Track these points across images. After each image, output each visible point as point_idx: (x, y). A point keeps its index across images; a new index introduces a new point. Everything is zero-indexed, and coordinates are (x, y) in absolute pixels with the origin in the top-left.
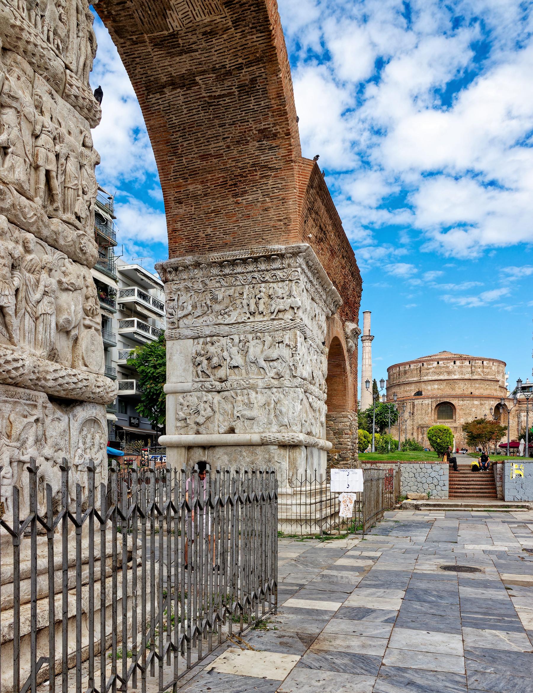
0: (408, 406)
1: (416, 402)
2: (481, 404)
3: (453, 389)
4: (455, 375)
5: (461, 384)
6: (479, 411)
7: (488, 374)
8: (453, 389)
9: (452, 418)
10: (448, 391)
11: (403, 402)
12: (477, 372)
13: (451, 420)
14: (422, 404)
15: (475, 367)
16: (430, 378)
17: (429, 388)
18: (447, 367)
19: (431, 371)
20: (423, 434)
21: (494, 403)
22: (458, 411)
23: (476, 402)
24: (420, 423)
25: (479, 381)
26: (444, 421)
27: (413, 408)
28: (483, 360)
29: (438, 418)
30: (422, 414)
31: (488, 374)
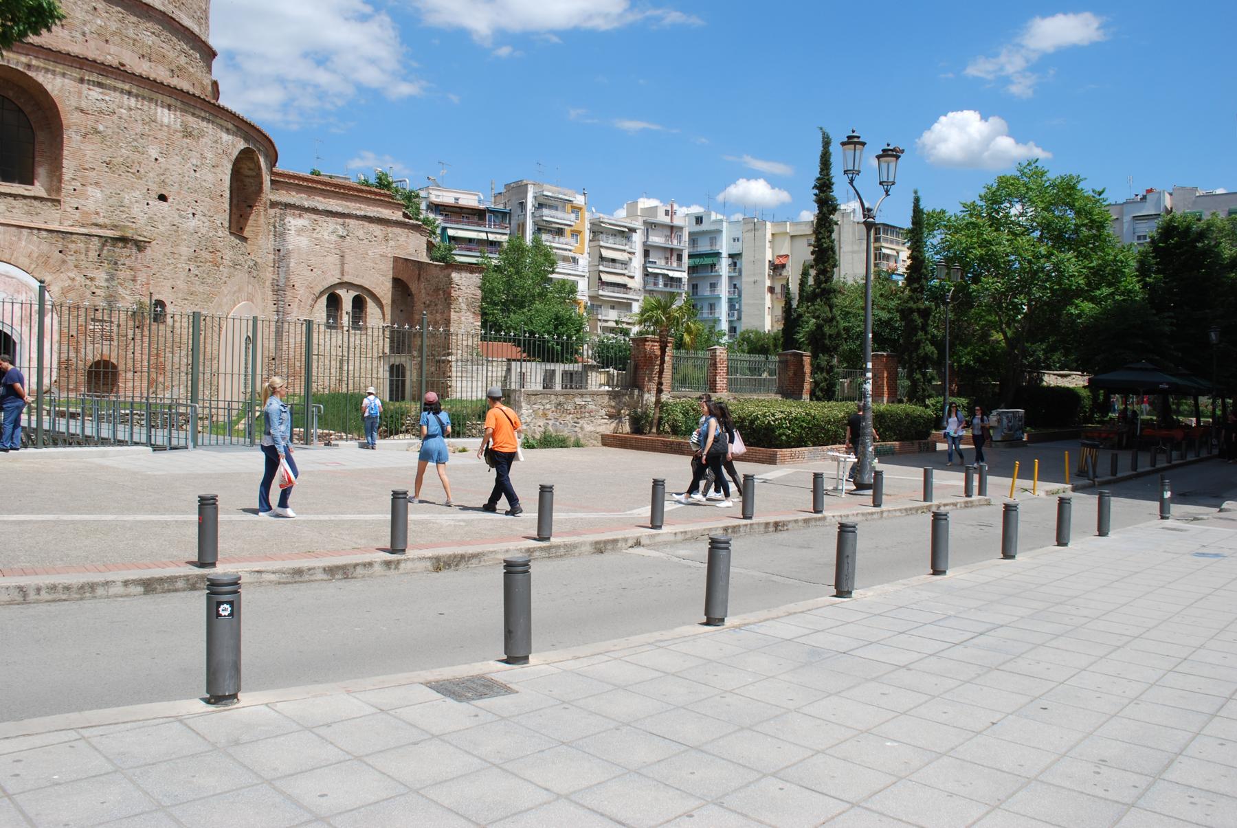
2: (187, 133)
23: (165, 116)
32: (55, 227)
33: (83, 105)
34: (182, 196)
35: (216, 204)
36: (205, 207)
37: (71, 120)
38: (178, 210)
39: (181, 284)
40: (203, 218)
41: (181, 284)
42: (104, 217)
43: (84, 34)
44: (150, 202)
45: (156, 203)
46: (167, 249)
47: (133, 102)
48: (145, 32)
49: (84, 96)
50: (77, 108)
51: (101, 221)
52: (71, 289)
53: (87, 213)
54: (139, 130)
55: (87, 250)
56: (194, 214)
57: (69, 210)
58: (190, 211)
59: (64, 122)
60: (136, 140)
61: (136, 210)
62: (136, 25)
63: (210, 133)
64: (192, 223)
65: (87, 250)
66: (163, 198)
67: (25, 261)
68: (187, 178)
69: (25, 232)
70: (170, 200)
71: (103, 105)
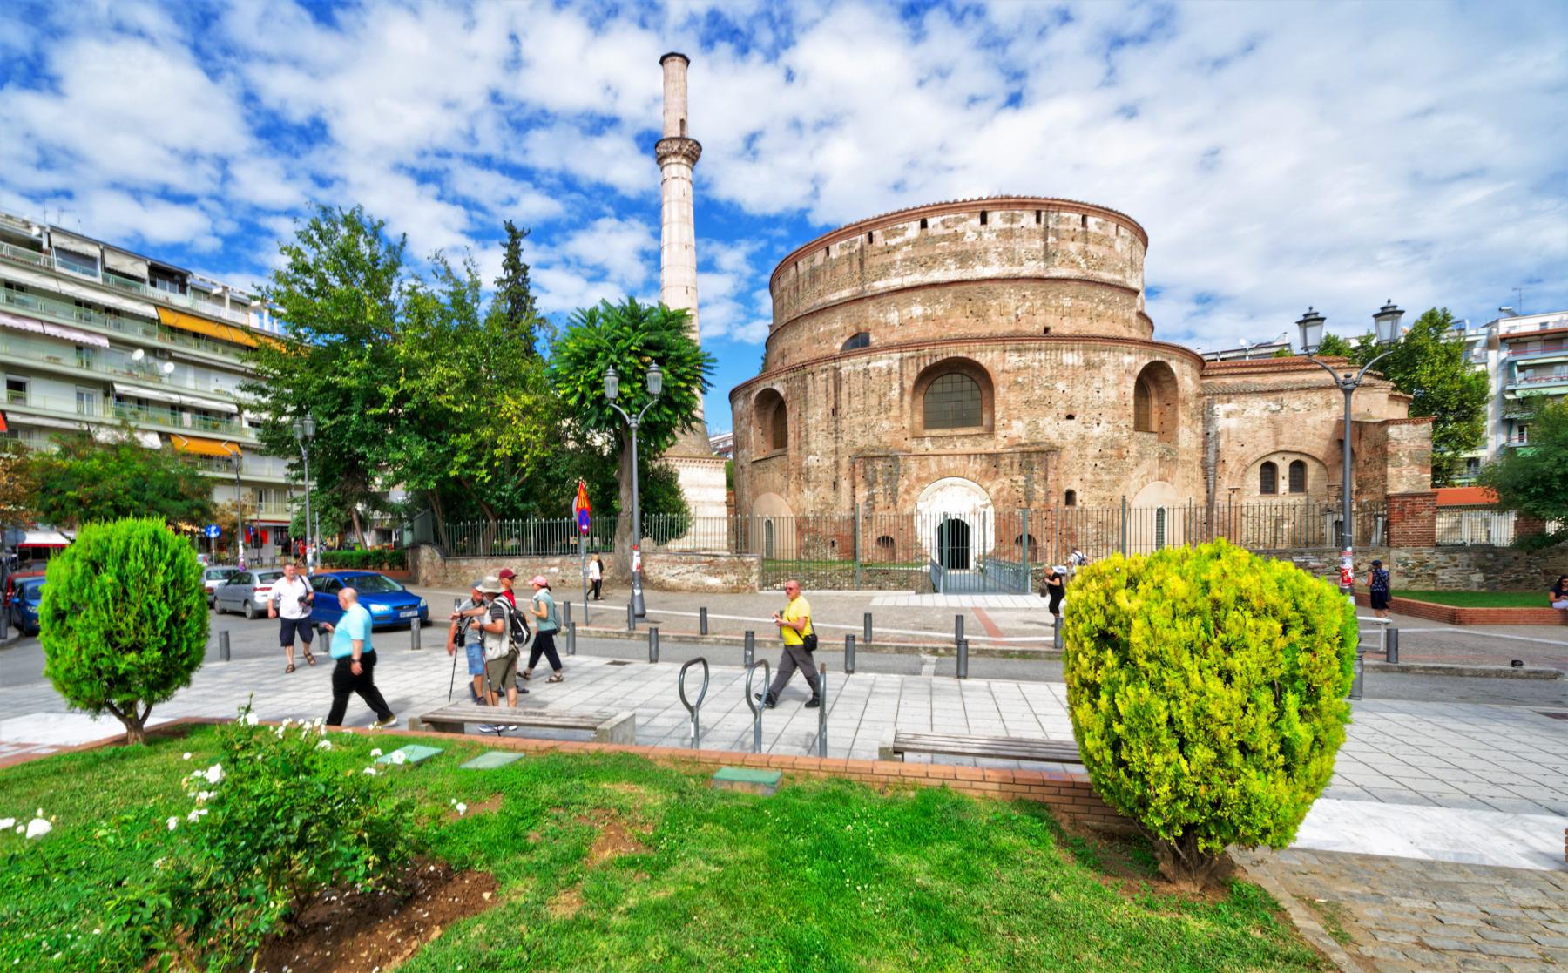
0: (821, 386)
1: (847, 367)
2: (1089, 365)
3: (980, 316)
4: (986, 264)
5: (1010, 298)
6: (1079, 393)
8: (980, 316)
9: (977, 422)
10: (962, 324)
11: (801, 370)
12: (1066, 254)
13: (973, 431)
14: (867, 372)
15: (1057, 233)
16: (895, 282)
17: (893, 317)
18: (957, 237)
20: (871, 484)
21: (1137, 361)
22: (1001, 392)
23: (1071, 358)
24: (861, 442)
25: (1074, 287)
26: (948, 432)
27: (837, 388)
28: (1085, 210)
29: (929, 424)
30: (866, 411)
32: (991, 450)
33: (1007, 368)
35: (1120, 412)
37: (999, 380)
39: (1088, 476)
41: (1088, 476)
43: (1017, 316)
46: (1075, 453)
47: (1043, 356)
51: (1023, 441)
52: (1002, 489)
54: (1048, 373)
55: (1012, 463)
58: (1095, 422)
59: (994, 382)
61: (1049, 430)
62: (1057, 297)
64: (1097, 431)
65: (1012, 463)
66: (1070, 417)
67: (972, 475)
71: (1021, 364)
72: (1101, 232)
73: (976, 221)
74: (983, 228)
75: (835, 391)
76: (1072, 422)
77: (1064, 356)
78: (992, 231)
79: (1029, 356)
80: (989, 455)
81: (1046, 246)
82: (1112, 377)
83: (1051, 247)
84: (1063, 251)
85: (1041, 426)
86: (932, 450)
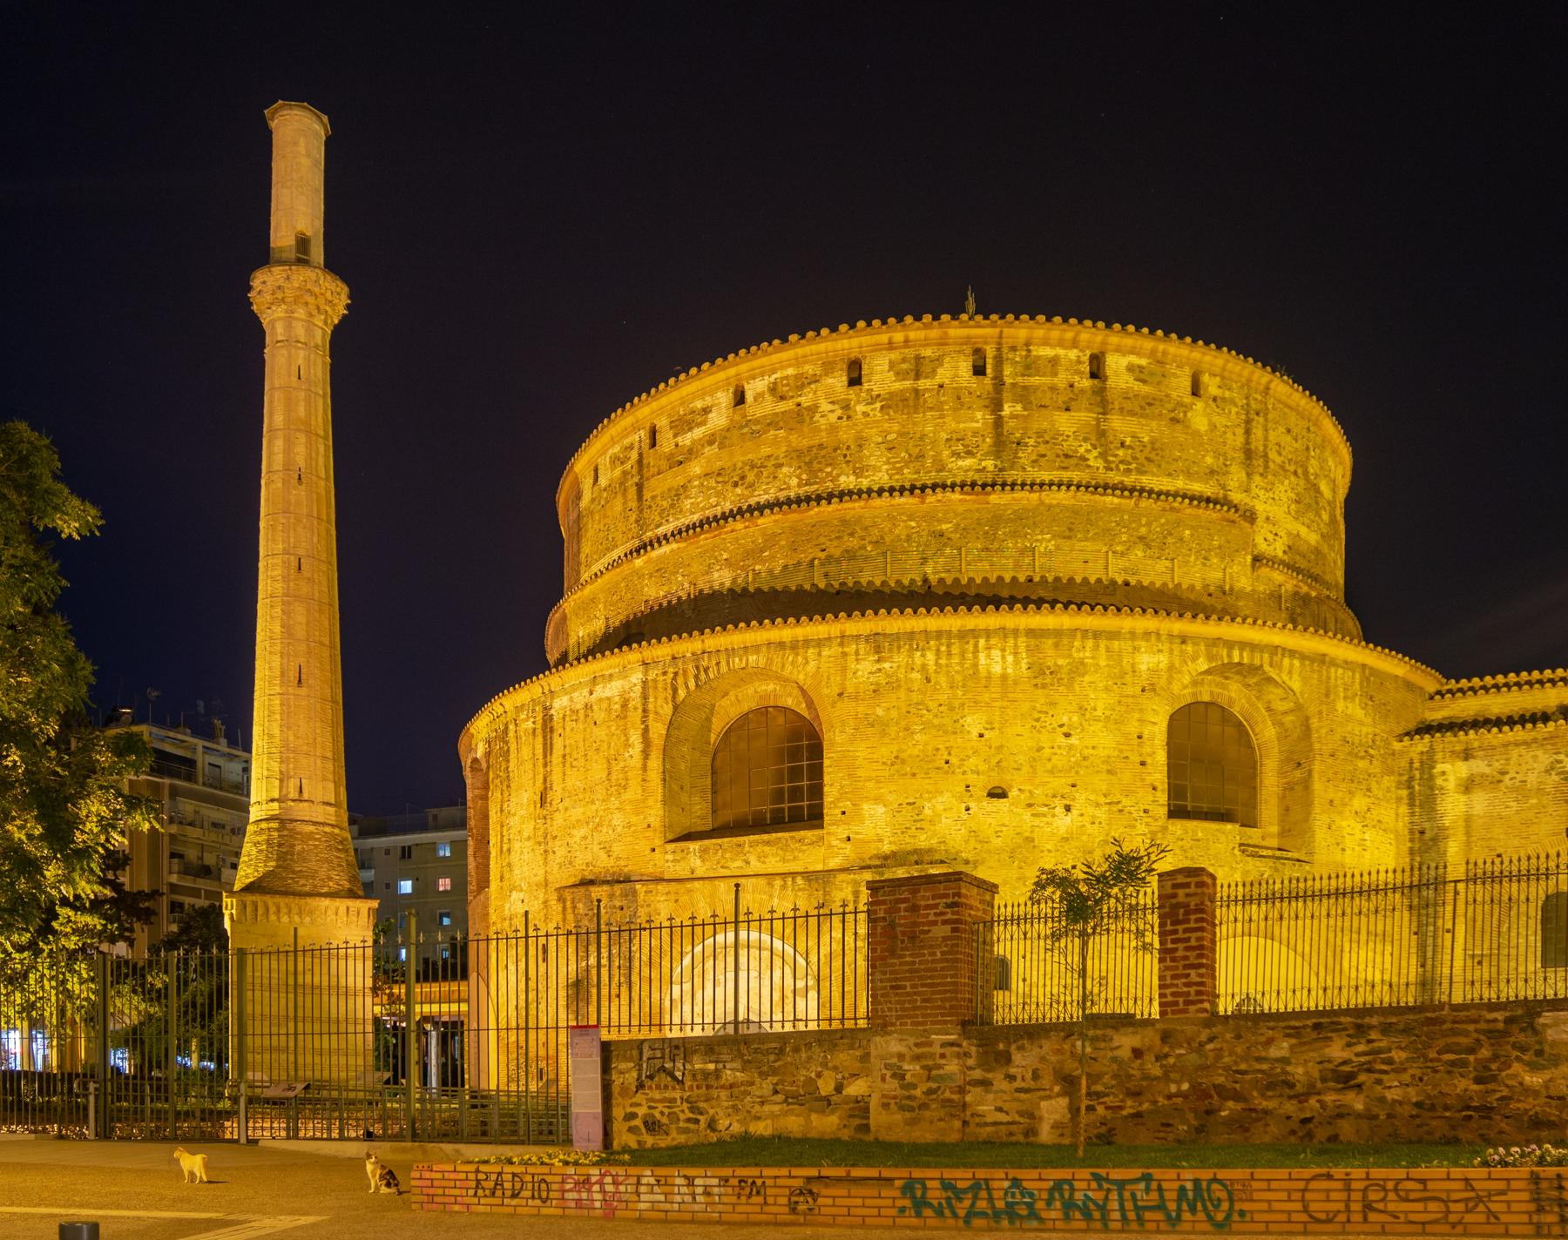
7: (1152, 455)
12: (1049, 438)
19: (696, 468)
23: (995, 661)
31: (1152, 455)
32: (819, 867)
34: (1037, 782)
36: (1094, 791)
38: (1030, 805)
40: (1091, 810)
42: (890, 843)
44: (972, 805)
45: (985, 804)
48: (1039, 537)
49: (849, 675)
50: (840, 695)
53: (863, 842)
56: (1068, 809)
57: (835, 843)
60: (936, 716)
63: (1103, 663)
64: (1063, 822)
66: (998, 794)
68: (1047, 751)
69: (778, 882)
70: (1013, 793)
72: (1145, 389)
73: (838, 381)
74: (852, 393)
75: (545, 756)
76: (1002, 804)
77: (982, 657)
78: (874, 399)
79: (900, 658)
80: (808, 875)
81: (998, 423)
82: (1101, 702)
83: (1010, 425)
84: (1039, 434)
85: (927, 812)
86: (699, 873)
